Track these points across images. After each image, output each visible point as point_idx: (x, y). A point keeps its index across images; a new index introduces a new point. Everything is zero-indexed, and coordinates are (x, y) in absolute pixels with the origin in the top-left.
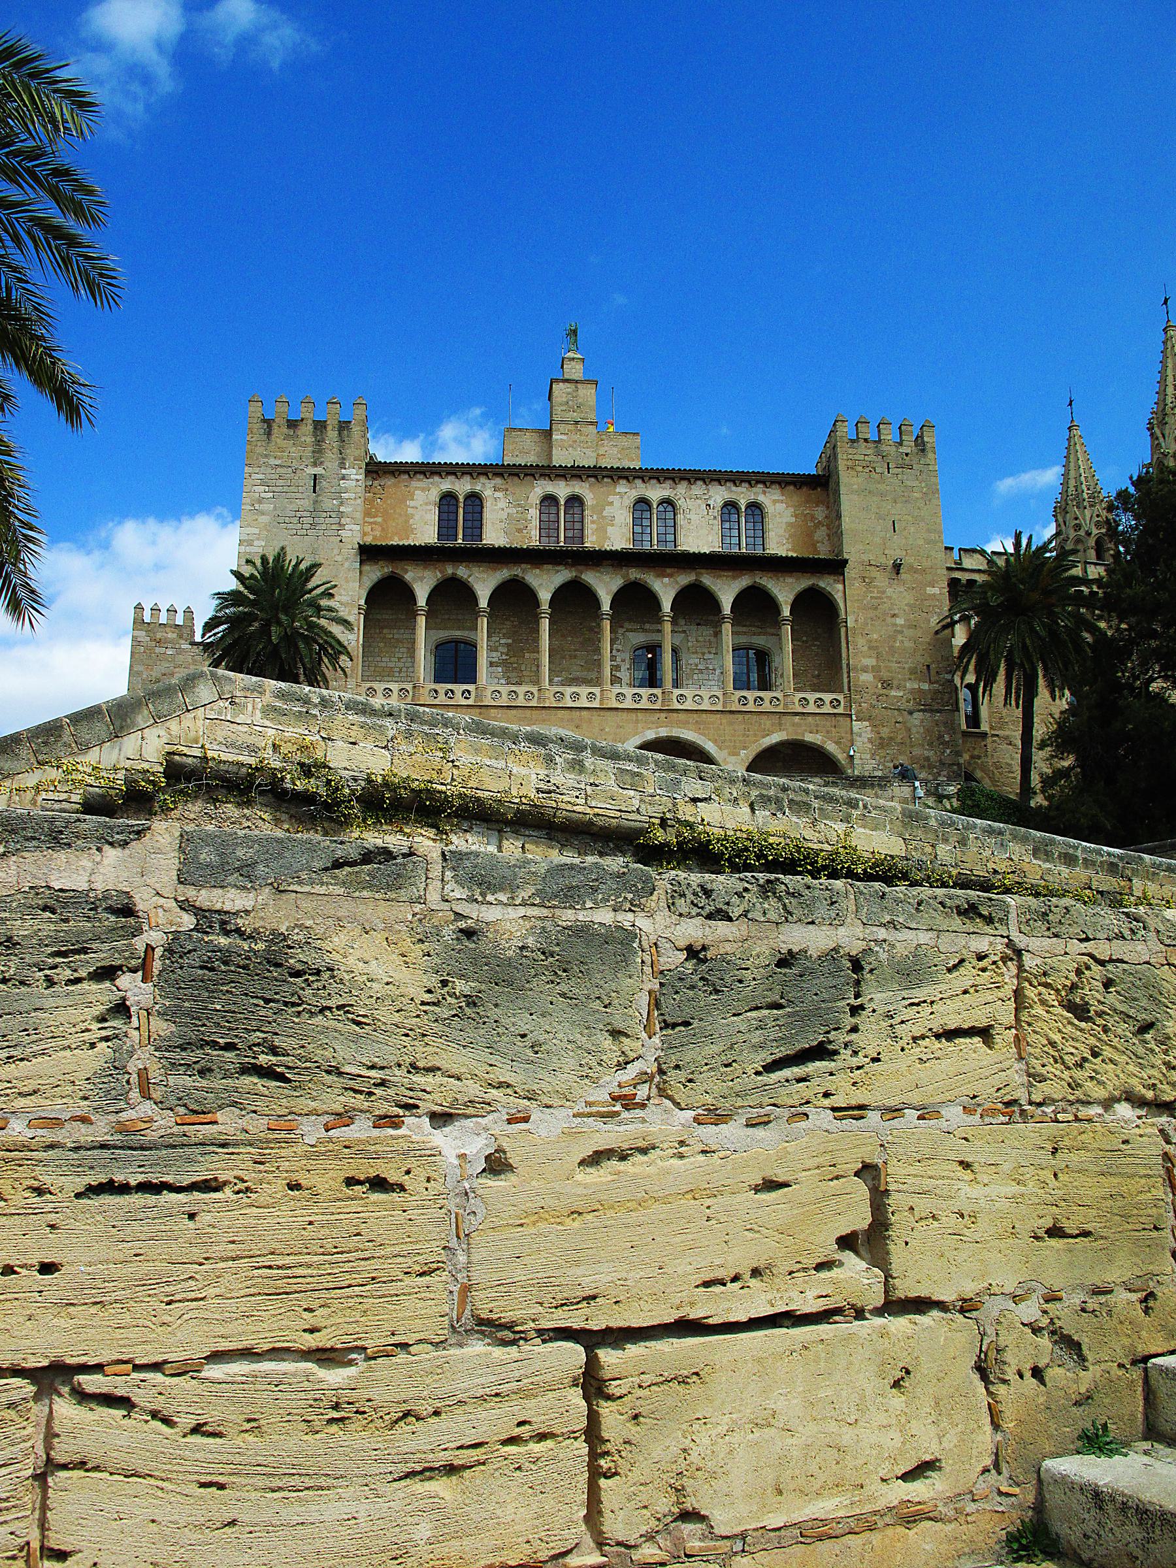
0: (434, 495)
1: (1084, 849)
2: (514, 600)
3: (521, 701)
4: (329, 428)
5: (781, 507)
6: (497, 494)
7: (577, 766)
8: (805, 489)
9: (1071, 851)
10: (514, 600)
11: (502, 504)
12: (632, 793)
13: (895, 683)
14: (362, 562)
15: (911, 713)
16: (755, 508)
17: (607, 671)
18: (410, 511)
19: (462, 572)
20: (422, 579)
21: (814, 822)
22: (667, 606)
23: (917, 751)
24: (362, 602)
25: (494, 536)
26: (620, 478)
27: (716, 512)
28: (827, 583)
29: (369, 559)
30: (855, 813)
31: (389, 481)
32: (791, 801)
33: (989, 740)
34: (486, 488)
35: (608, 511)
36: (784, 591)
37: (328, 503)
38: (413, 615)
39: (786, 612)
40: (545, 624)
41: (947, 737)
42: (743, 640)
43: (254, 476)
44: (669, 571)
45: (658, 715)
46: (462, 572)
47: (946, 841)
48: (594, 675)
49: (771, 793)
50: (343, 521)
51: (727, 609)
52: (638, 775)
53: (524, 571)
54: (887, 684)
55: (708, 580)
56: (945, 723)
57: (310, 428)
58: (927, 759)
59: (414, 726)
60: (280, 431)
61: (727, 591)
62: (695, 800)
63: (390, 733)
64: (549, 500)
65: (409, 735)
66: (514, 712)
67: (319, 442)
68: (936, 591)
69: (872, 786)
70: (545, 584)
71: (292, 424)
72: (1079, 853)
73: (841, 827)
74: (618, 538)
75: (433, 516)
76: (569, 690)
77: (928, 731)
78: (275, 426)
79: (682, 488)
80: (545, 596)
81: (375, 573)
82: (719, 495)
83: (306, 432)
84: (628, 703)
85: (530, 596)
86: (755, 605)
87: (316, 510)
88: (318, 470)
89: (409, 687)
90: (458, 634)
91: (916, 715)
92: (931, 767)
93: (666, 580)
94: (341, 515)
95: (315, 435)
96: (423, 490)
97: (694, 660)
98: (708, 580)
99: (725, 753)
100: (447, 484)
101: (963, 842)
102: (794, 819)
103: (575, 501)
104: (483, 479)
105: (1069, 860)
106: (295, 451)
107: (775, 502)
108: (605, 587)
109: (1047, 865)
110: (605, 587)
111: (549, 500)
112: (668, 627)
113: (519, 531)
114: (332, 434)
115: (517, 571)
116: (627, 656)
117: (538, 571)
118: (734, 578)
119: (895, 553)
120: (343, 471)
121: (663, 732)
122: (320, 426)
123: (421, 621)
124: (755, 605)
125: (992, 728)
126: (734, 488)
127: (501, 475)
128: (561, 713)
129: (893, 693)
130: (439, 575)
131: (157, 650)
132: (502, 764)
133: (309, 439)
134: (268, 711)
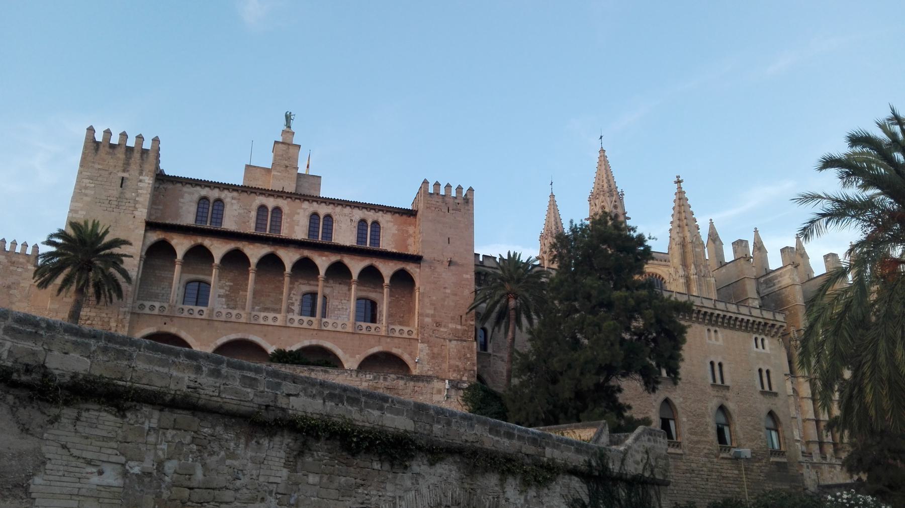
0: (196, 197)
1: (519, 430)
2: (236, 259)
3: (233, 319)
4: (135, 152)
5: (391, 225)
6: (234, 201)
7: (216, 373)
8: (405, 217)
9: (511, 431)
10: (236, 259)
12: (249, 390)
13: (443, 324)
14: (146, 231)
15: (450, 341)
16: (376, 224)
17: (284, 306)
18: (181, 205)
19: (207, 242)
20: (182, 244)
21: (361, 410)
22: (322, 272)
23: (452, 362)
24: (144, 254)
25: (229, 224)
26: (305, 200)
27: (356, 224)
28: (411, 268)
29: (151, 230)
30: (386, 405)
31: (170, 186)
32: (348, 398)
33: (492, 358)
34: (226, 196)
35: (296, 217)
36: (387, 269)
37: (129, 194)
38: (173, 264)
39: (387, 281)
40: (252, 276)
41: (468, 355)
42: (363, 294)
43: (84, 173)
44: (326, 253)
45: (312, 332)
46: (207, 242)
47: (438, 422)
48: (277, 307)
49: (337, 392)
50: (137, 206)
51: (355, 276)
52: (255, 379)
53: (244, 246)
54: (438, 324)
55: (348, 260)
56: (468, 348)
57: (123, 150)
58: (458, 366)
59: (110, 345)
61: (356, 266)
62: (289, 395)
63: (93, 348)
64: (262, 208)
65: (105, 350)
66: (229, 325)
68: (468, 276)
69: (423, 381)
70: (255, 253)
71: (113, 146)
72: (516, 432)
73: (376, 413)
74: (300, 233)
75: (193, 209)
76: (263, 314)
77: (459, 351)
78: (101, 147)
79: (338, 209)
80: (254, 261)
81: (154, 237)
82: (358, 214)
84: (296, 324)
86: (371, 275)
87: (120, 198)
88: (125, 175)
89: (166, 305)
90: (201, 277)
91: (454, 342)
92: (459, 371)
93: (324, 258)
94: (136, 202)
95: (126, 155)
96: (190, 193)
97: (336, 303)
98: (348, 260)
99: (348, 356)
100: (205, 192)
101: (449, 424)
102: (349, 408)
103: (277, 210)
104: (226, 192)
105: (509, 435)
107: (388, 222)
108: (289, 257)
109: (497, 438)
110: (289, 257)
111: (262, 208)
112: (321, 283)
113: (244, 223)
114: (137, 155)
116: (299, 298)
117: (251, 247)
118: (361, 261)
119: (448, 255)
120: (141, 178)
121: (314, 342)
123: (178, 268)
124: (371, 275)
125: (494, 351)
126: (366, 212)
127: (237, 191)
128: (257, 327)
129: (442, 329)
130: (193, 243)
131: (11, 268)
132: (166, 370)
134: (8, 330)
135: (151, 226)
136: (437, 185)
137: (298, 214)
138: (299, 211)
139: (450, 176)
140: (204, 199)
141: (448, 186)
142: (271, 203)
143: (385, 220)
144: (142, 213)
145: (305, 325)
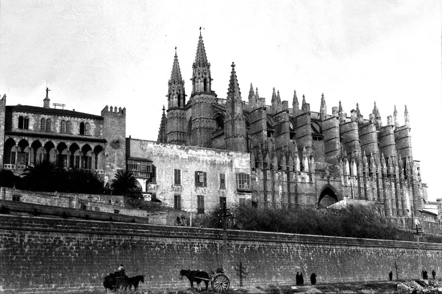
5: (93, 124)
6: (33, 118)
11: (33, 120)
27: (79, 125)
28: (102, 145)
34: (30, 116)
35: (56, 123)
55: (78, 143)
98: (78, 143)
107: (92, 123)
126: (84, 119)
136: (111, 108)
137: (57, 122)
138: (57, 120)
139: (116, 103)
141: (116, 108)
142: (46, 117)
143: (91, 122)
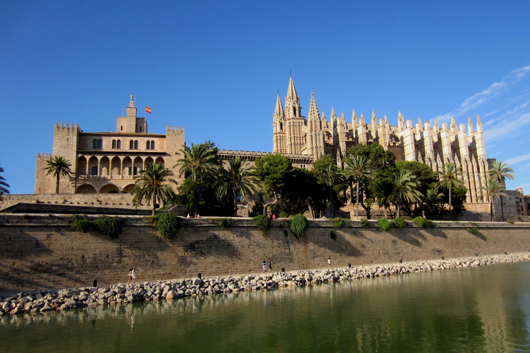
0: (92, 140)
2: (105, 160)
10: (105, 160)
31: (84, 137)
60: (61, 129)
61: (144, 158)
67: (68, 131)
70: (111, 158)
71: (63, 128)
82: (146, 139)
83: (66, 130)
85: (108, 159)
87: (67, 144)
100: (95, 138)
103: (119, 141)
106: (64, 133)
108: (122, 158)
110: (122, 158)
114: (71, 130)
115: (106, 155)
122: (69, 129)
133: (67, 131)
135: (78, 153)
140: (95, 140)
142: (116, 139)
144: (75, 148)
145: (128, 178)
